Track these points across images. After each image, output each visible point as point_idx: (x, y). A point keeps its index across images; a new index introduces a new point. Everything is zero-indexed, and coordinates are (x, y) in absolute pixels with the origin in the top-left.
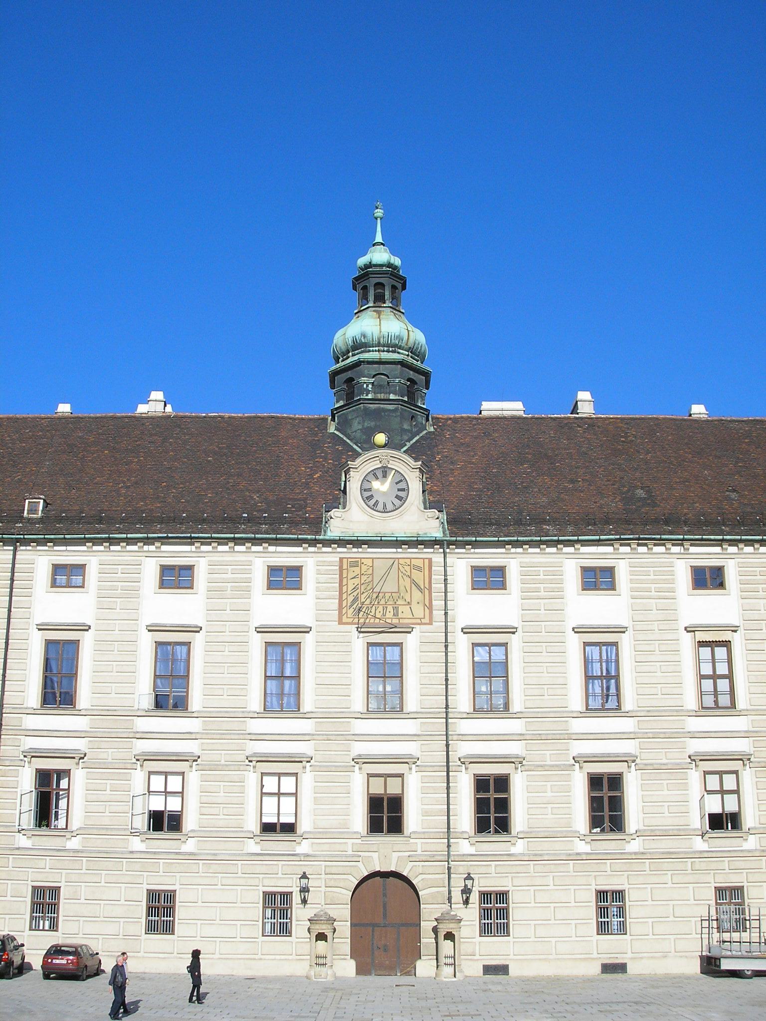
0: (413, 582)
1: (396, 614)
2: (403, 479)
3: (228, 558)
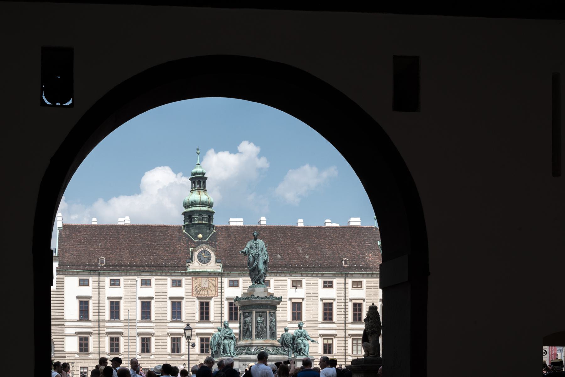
0: (212, 284)
1: (208, 293)
2: (210, 254)
3: (160, 277)
